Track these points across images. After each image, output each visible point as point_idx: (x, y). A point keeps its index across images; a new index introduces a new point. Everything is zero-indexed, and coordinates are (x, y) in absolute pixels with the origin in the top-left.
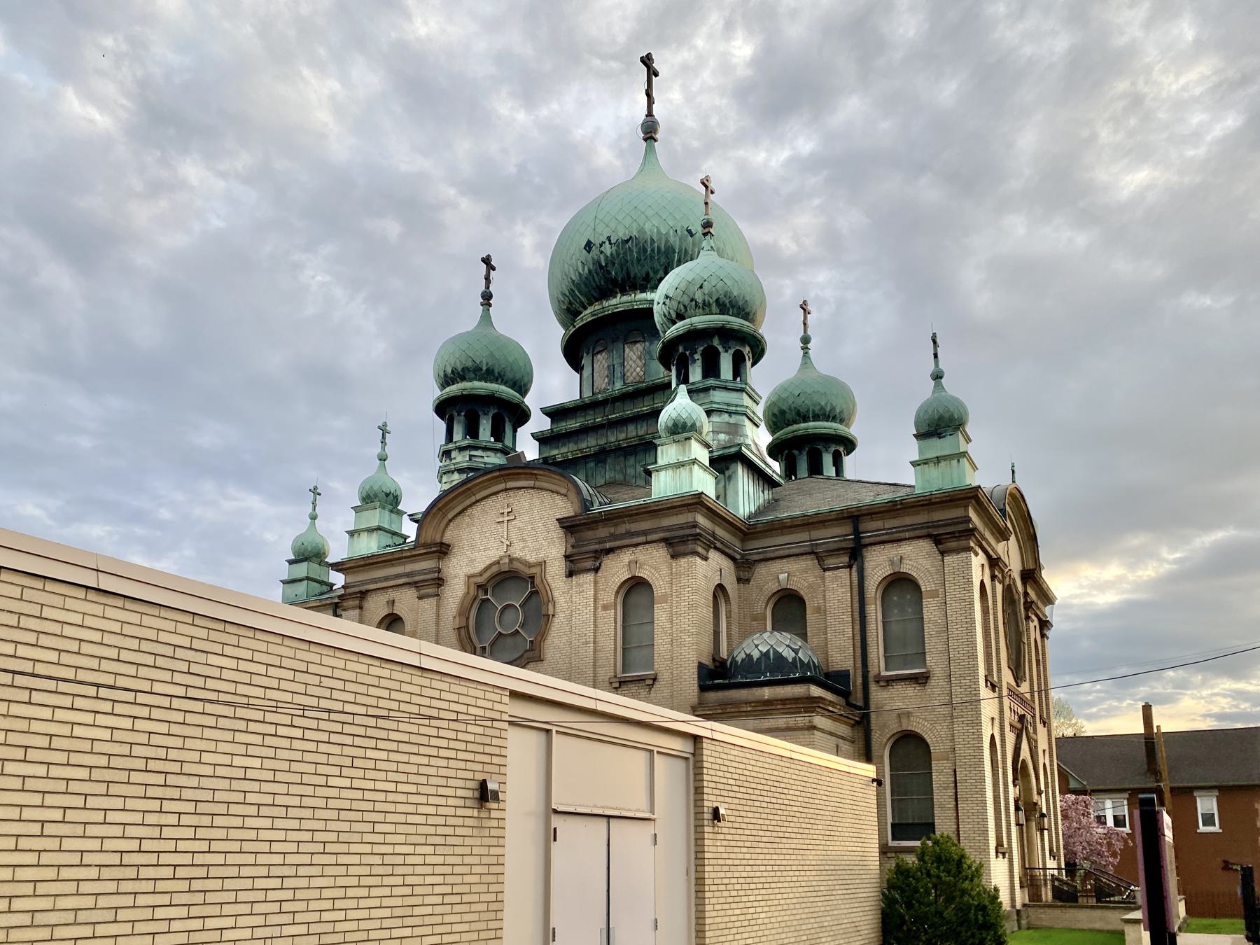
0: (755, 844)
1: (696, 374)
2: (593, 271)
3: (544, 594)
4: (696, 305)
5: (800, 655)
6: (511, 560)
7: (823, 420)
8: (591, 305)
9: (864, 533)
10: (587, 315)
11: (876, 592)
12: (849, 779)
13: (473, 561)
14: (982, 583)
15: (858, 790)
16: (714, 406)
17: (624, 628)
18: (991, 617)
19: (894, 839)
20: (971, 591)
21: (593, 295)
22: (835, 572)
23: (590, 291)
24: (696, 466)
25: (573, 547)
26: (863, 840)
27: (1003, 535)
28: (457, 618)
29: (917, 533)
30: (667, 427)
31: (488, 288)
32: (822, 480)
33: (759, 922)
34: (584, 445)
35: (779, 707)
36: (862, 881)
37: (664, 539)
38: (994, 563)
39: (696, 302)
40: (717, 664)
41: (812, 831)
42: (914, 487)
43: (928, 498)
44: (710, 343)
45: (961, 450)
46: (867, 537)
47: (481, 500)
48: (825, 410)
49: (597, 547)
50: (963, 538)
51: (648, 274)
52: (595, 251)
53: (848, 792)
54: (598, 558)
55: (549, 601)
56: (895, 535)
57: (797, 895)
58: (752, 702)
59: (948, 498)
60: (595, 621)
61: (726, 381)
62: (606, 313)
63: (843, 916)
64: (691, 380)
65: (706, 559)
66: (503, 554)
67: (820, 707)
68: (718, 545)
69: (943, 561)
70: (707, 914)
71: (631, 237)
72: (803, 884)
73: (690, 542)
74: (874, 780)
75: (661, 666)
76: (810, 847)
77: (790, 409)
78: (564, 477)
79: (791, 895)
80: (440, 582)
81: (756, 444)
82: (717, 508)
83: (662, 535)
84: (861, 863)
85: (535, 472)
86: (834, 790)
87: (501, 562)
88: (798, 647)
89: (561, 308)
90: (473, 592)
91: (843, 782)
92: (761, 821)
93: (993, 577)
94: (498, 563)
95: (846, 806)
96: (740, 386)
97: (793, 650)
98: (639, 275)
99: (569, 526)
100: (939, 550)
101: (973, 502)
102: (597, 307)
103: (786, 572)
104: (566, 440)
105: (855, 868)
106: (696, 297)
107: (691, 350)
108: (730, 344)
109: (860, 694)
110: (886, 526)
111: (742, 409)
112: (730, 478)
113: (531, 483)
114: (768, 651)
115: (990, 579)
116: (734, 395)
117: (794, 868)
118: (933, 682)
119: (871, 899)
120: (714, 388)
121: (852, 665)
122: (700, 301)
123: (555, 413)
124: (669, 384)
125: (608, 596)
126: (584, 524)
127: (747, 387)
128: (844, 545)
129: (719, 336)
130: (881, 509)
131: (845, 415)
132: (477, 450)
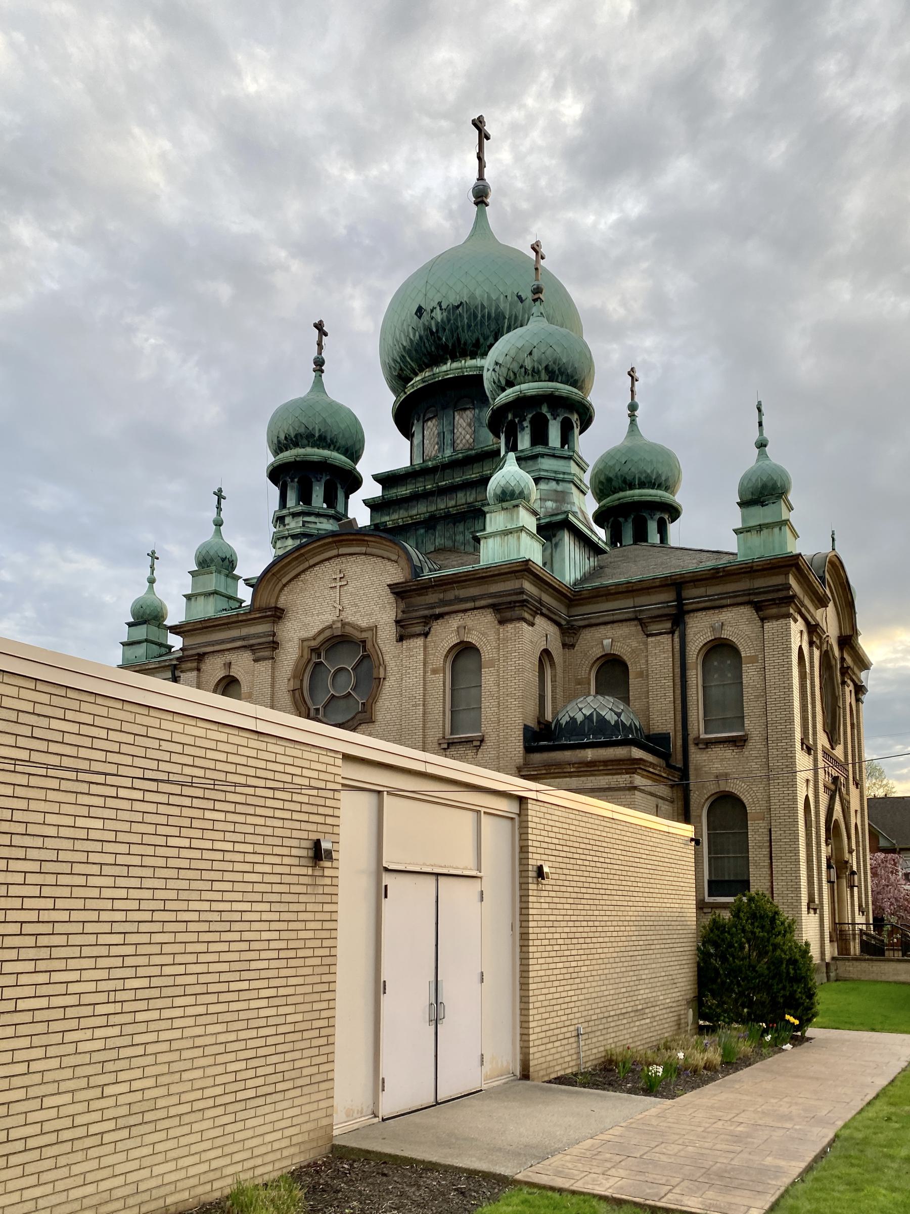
0: (577, 901)
1: (524, 442)
2: (424, 338)
3: (375, 657)
4: (526, 372)
5: (622, 718)
6: (344, 624)
7: (648, 488)
8: (421, 370)
9: (685, 600)
10: (417, 382)
11: (697, 658)
12: (668, 838)
13: (305, 625)
14: (800, 648)
15: (677, 849)
16: (542, 473)
17: (452, 690)
18: (808, 682)
20: (789, 657)
21: (423, 361)
22: (658, 638)
23: (421, 359)
24: (523, 535)
25: (403, 612)
26: (680, 897)
27: (822, 602)
28: (292, 680)
29: (739, 600)
30: (495, 495)
31: (321, 354)
32: (647, 548)
33: (581, 975)
34: (414, 512)
35: (601, 768)
36: (679, 936)
37: (492, 605)
38: (813, 629)
39: (526, 369)
40: (542, 726)
41: (632, 889)
42: (736, 554)
43: (750, 565)
44: (539, 410)
45: (783, 518)
46: (689, 604)
47: (314, 565)
48: (650, 477)
49: (426, 612)
51: (478, 340)
52: (426, 317)
53: (667, 851)
54: (428, 624)
55: (380, 664)
57: (617, 949)
58: (575, 763)
59: (770, 566)
60: (425, 684)
61: (554, 449)
62: (437, 379)
63: (661, 969)
64: (520, 447)
65: (532, 624)
66: (335, 618)
67: (640, 768)
68: (544, 611)
69: (763, 627)
70: (531, 968)
71: (461, 303)
72: (623, 939)
73: (516, 609)
74: (692, 840)
75: (487, 727)
76: (630, 904)
77: (616, 476)
78: (395, 544)
79: (612, 950)
80: (274, 645)
81: (582, 512)
82: (544, 575)
83: (490, 601)
84: (679, 919)
85: (366, 538)
86: (654, 849)
87: (334, 627)
88: (620, 711)
89: (392, 374)
90: (306, 654)
91: (662, 841)
92: (583, 879)
93: (811, 643)
94: (330, 627)
95: (665, 864)
97: (616, 713)
98: (469, 341)
99: (399, 592)
100: (759, 617)
101: (794, 569)
102: (427, 374)
103: (609, 638)
104: (397, 507)
105: (673, 923)
106: (526, 364)
107: (520, 418)
109: (679, 756)
110: (708, 594)
112: (556, 545)
113: (363, 549)
114: (592, 714)
115: (808, 646)
117: (615, 923)
118: (750, 744)
119: (687, 953)
120: (543, 455)
121: (673, 728)
122: (529, 367)
123: (386, 480)
124: (499, 451)
125: (438, 658)
126: (414, 590)
127: (575, 455)
128: (667, 611)
130: (704, 577)
131: (670, 483)
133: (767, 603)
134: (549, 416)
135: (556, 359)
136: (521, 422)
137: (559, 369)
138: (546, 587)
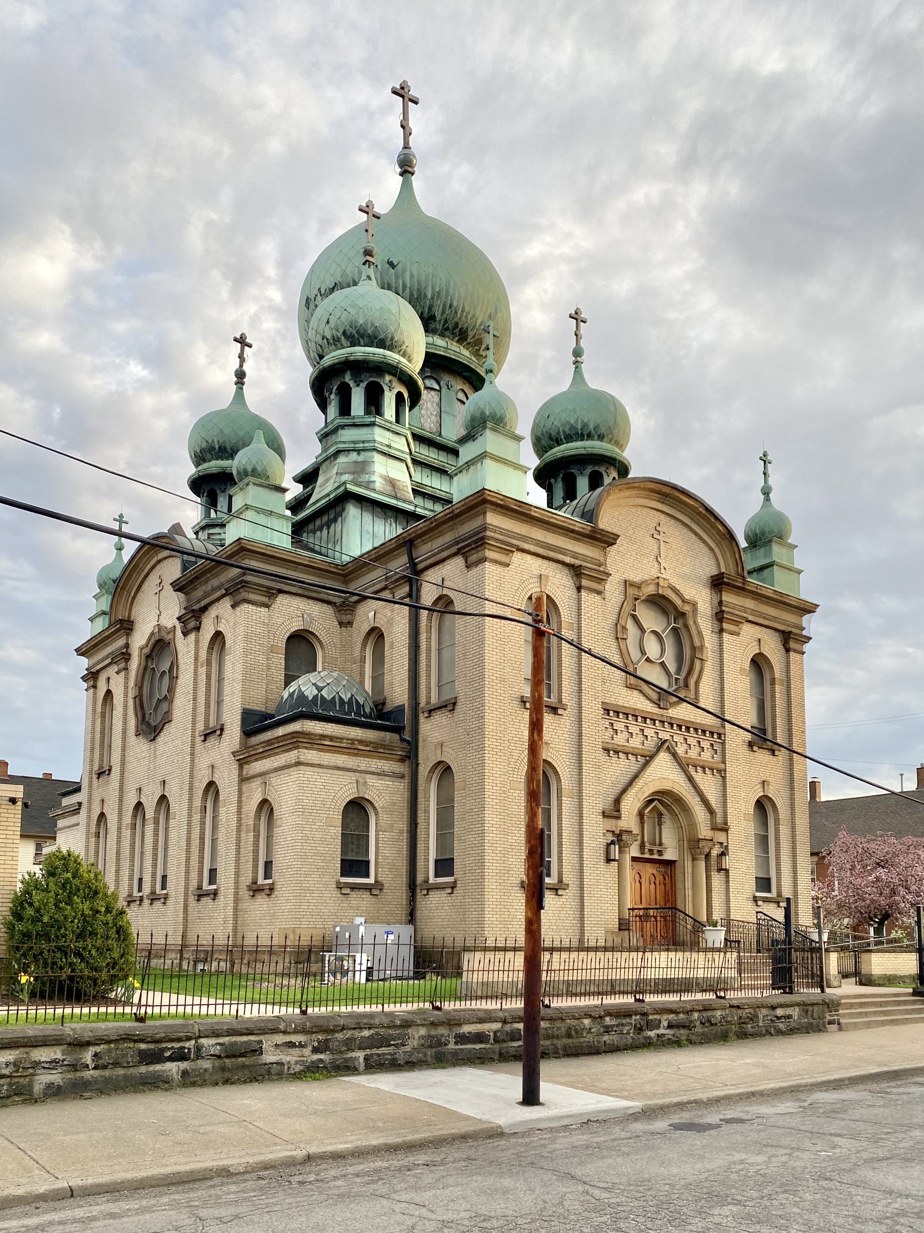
5: (324, 693)
19: (437, 875)
56: (439, 556)
73: (241, 590)
82: (276, 552)
108: (363, 376)
111: (372, 445)
116: (364, 431)
118: (458, 708)
120: (343, 427)
133: (467, 549)
134: (352, 384)
135: (352, 322)
136: (329, 397)
138: (294, 565)
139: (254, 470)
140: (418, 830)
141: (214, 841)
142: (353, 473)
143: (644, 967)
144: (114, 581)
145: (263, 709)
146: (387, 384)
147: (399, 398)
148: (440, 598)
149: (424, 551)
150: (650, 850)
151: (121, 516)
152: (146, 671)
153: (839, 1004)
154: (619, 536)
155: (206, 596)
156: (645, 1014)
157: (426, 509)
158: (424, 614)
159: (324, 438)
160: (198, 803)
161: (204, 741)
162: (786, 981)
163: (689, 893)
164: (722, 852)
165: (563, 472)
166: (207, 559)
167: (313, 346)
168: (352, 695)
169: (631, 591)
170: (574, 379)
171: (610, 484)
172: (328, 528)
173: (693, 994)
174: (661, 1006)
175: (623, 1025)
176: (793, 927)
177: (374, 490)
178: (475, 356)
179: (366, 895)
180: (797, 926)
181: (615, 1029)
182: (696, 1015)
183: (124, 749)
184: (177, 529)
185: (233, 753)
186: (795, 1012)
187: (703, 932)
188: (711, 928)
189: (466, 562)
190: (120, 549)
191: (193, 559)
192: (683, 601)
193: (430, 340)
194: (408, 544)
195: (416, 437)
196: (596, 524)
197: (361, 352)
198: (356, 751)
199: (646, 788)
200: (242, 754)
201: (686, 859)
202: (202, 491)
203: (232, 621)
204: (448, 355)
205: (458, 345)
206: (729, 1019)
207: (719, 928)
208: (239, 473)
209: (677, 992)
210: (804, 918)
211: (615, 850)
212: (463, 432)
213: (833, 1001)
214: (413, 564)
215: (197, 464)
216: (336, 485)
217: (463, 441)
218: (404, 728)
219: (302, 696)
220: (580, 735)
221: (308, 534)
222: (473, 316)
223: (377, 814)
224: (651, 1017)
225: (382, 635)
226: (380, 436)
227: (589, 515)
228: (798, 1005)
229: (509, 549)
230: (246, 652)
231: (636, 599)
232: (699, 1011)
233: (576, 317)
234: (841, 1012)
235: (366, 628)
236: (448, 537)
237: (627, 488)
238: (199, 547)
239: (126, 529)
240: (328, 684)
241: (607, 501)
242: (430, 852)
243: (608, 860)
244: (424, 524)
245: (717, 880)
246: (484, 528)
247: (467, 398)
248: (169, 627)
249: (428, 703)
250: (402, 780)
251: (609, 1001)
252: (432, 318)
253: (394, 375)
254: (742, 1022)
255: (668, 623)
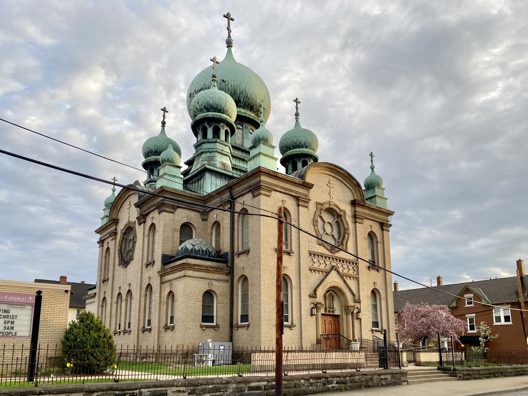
4: (198, 111)
7: (297, 148)
9: (233, 194)
16: (203, 150)
39: (198, 109)
50: (258, 190)
56: (242, 193)
71: (201, 88)
73: (162, 207)
96: (214, 140)
108: (212, 124)
110: (240, 190)
111: (215, 150)
116: (213, 144)
120: (204, 143)
129: (207, 121)
132: (152, 182)
134: (207, 126)
136: (199, 132)
137: (210, 107)
139: (168, 160)
140: (234, 303)
141: (150, 308)
142: (208, 161)
143: (326, 358)
144: (111, 204)
145: (171, 254)
146: (222, 127)
147: (226, 132)
148: (243, 209)
149: (236, 191)
150: (329, 311)
151: (115, 178)
152: (124, 239)
153: (407, 374)
154: (314, 185)
155: (148, 209)
156: (327, 378)
157: (237, 174)
158: (236, 215)
159: (196, 147)
160: (143, 292)
161: (146, 267)
162: (385, 364)
163: (345, 328)
164: (358, 311)
165: (292, 160)
166: (150, 194)
167: (192, 112)
168: (207, 248)
169: (319, 206)
170: (296, 125)
171: (310, 165)
172: (198, 182)
173: (347, 370)
174: (333, 375)
175: (318, 382)
176: (387, 342)
177: (216, 167)
178: (256, 116)
179: (212, 330)
180: (389, 341)
181: (314, 384)
182: (348, 378)
183: (114, 271)
184: (137, 183)
185: (158, 272)
186: (389, 377)
187: (351, 344)
188: (354, 342)
189: (253, 195)
190: (114, 191)
191: (142, 194)
192: (340, 210)
193: (239, 110)
194: (230, 188)
195: (233, 147)
196: (305, 180)
197: (211, 114)
198: (208, 271)
199: (327, 285)
200: (162, 273)
201: (344, 314)
202: (147, 168)
203: (158, 219)
204: (246, 116)
205: (250, 112)
206: (362, 380)
207: (357, 342)
208: (162, 161)
209: (340, 369)
210: (392, 338)
211: (315, 310)
212: (251, 145)
213: (404, 372)
214: (232, 196)
215: (146, 157)
216: (201, 165)
217: (251, 148)
218: (228, 261)
219: (186, 249)
220: (300, 264)
221: (190, 184)
222: (256, 101)
223: (217, 297)
224: (329, 379)
225: (220, 224)
226: (219, 147)
227: (302, 177)
228: (390, 374)
229: (270, 190)
230: (164, 232)
231: (321, 210)
232: (349, 376)
233: (296, 101)
234: (408, 377)
235: (213, 221)
236: (246, 185)
237: (317, 167)
238: (145, 189)
239: (116, 182)
240: (197, 244)
241: (309, 171)
242: (239, 312)
243: (312, 315)
244: (236, 180)
245: (356, 322)
246: (260, 182)
247: (253, 131)
248: (133, 221)
249: (238, 251)
250: (227, 283)
251: (312, 372)
252: (240, 101)
253: (224, 123)
254: (367, 381)
255: (334, 219)
